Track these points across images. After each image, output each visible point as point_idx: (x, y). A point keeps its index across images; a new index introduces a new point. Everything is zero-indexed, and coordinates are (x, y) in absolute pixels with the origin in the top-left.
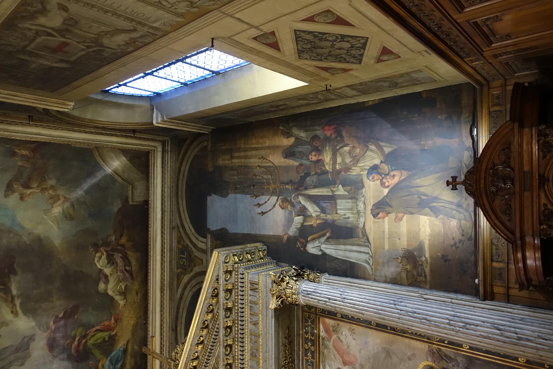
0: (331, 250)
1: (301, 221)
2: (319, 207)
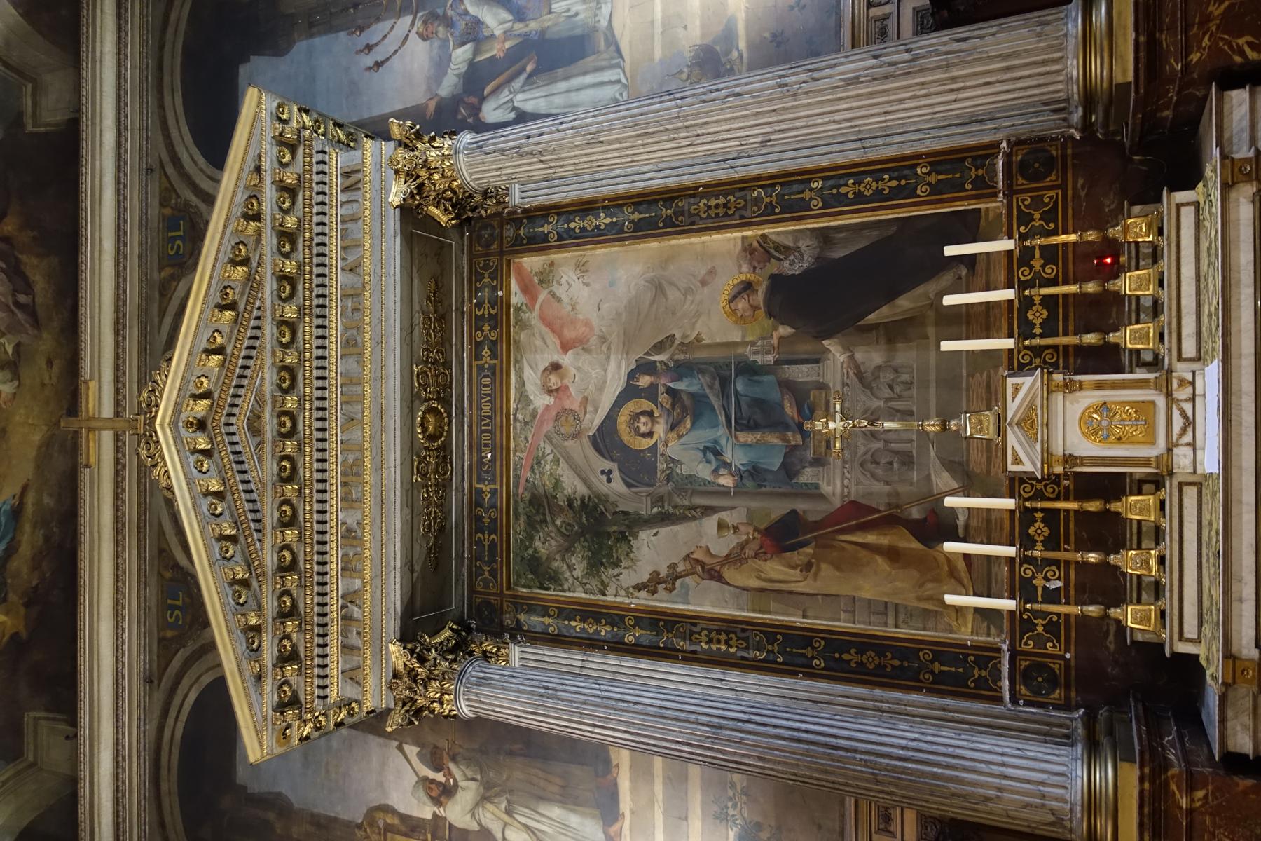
1: (469, 55)
2: (510, 10)
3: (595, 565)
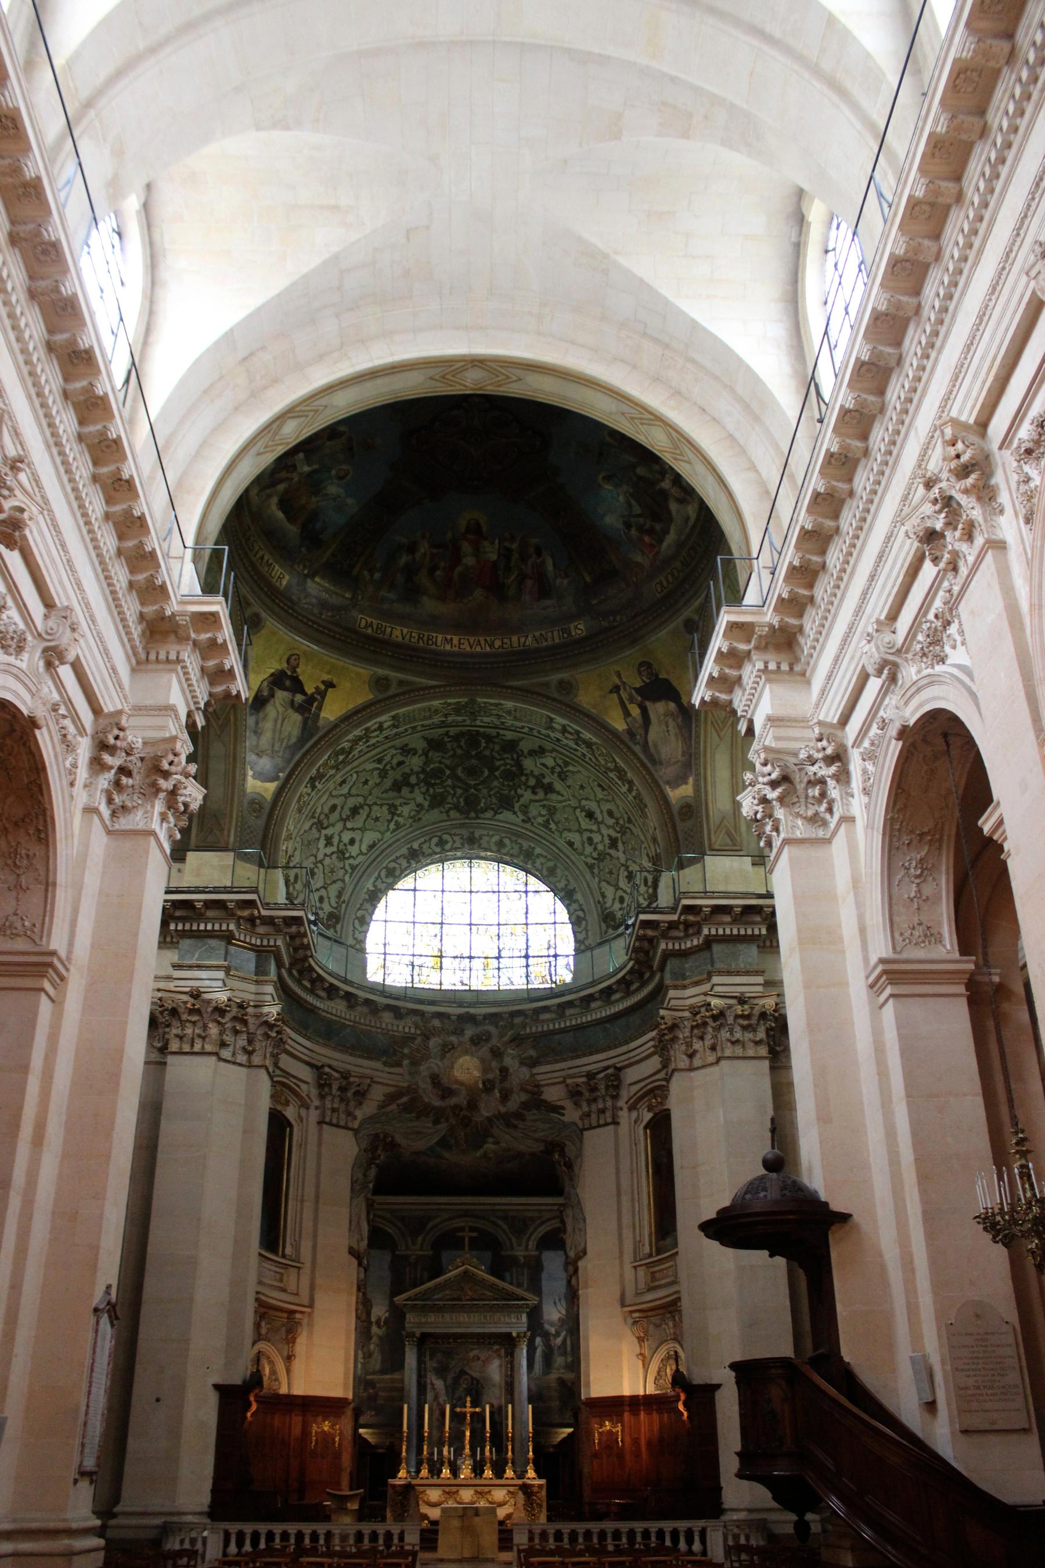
0: (539, 1353)
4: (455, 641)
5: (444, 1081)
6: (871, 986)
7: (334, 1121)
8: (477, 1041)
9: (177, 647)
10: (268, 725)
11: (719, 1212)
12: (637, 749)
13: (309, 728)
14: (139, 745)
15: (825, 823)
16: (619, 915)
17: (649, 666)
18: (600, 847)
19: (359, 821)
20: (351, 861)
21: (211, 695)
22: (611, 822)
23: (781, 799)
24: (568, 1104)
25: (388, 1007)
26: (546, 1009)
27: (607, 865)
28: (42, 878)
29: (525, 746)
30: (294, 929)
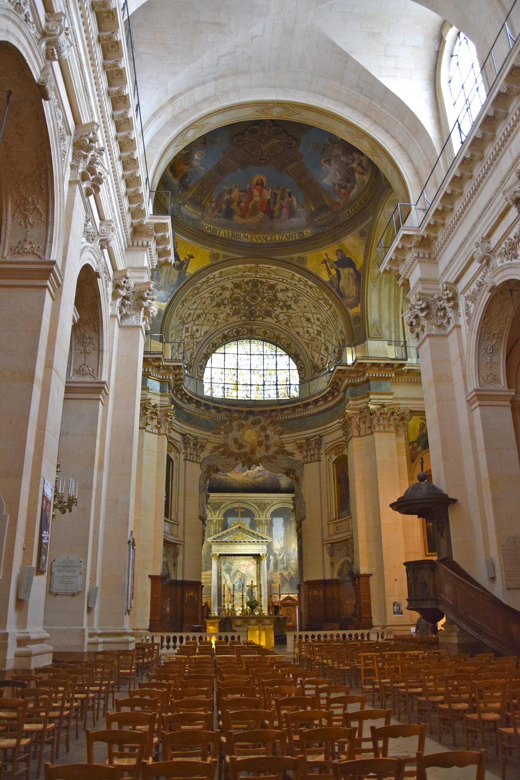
3: (225, 570)
4: (249, 237)
5: (240, 441)
6: (468, 401)
7: (191, 459)
8: (254, 423)
9: (147, 239)
10: (163, 275)
11: (398, 499)
12: (334, 290)
13: (181, 277)
14: (133, 286)
15: (445, 328)
16: (321, 366)
17: (341, 251)
18: (312, 335)
19: (200, 321)
20: (197, 340)
21: (158, 262)
22: (318, 323)
23: (426, 317)
24: (297, 452)
25: (215, 408)
26: (287, 409)
27: (316, 342)
28: (96, 348)
29: (279, 287)
30: (178, 371)
